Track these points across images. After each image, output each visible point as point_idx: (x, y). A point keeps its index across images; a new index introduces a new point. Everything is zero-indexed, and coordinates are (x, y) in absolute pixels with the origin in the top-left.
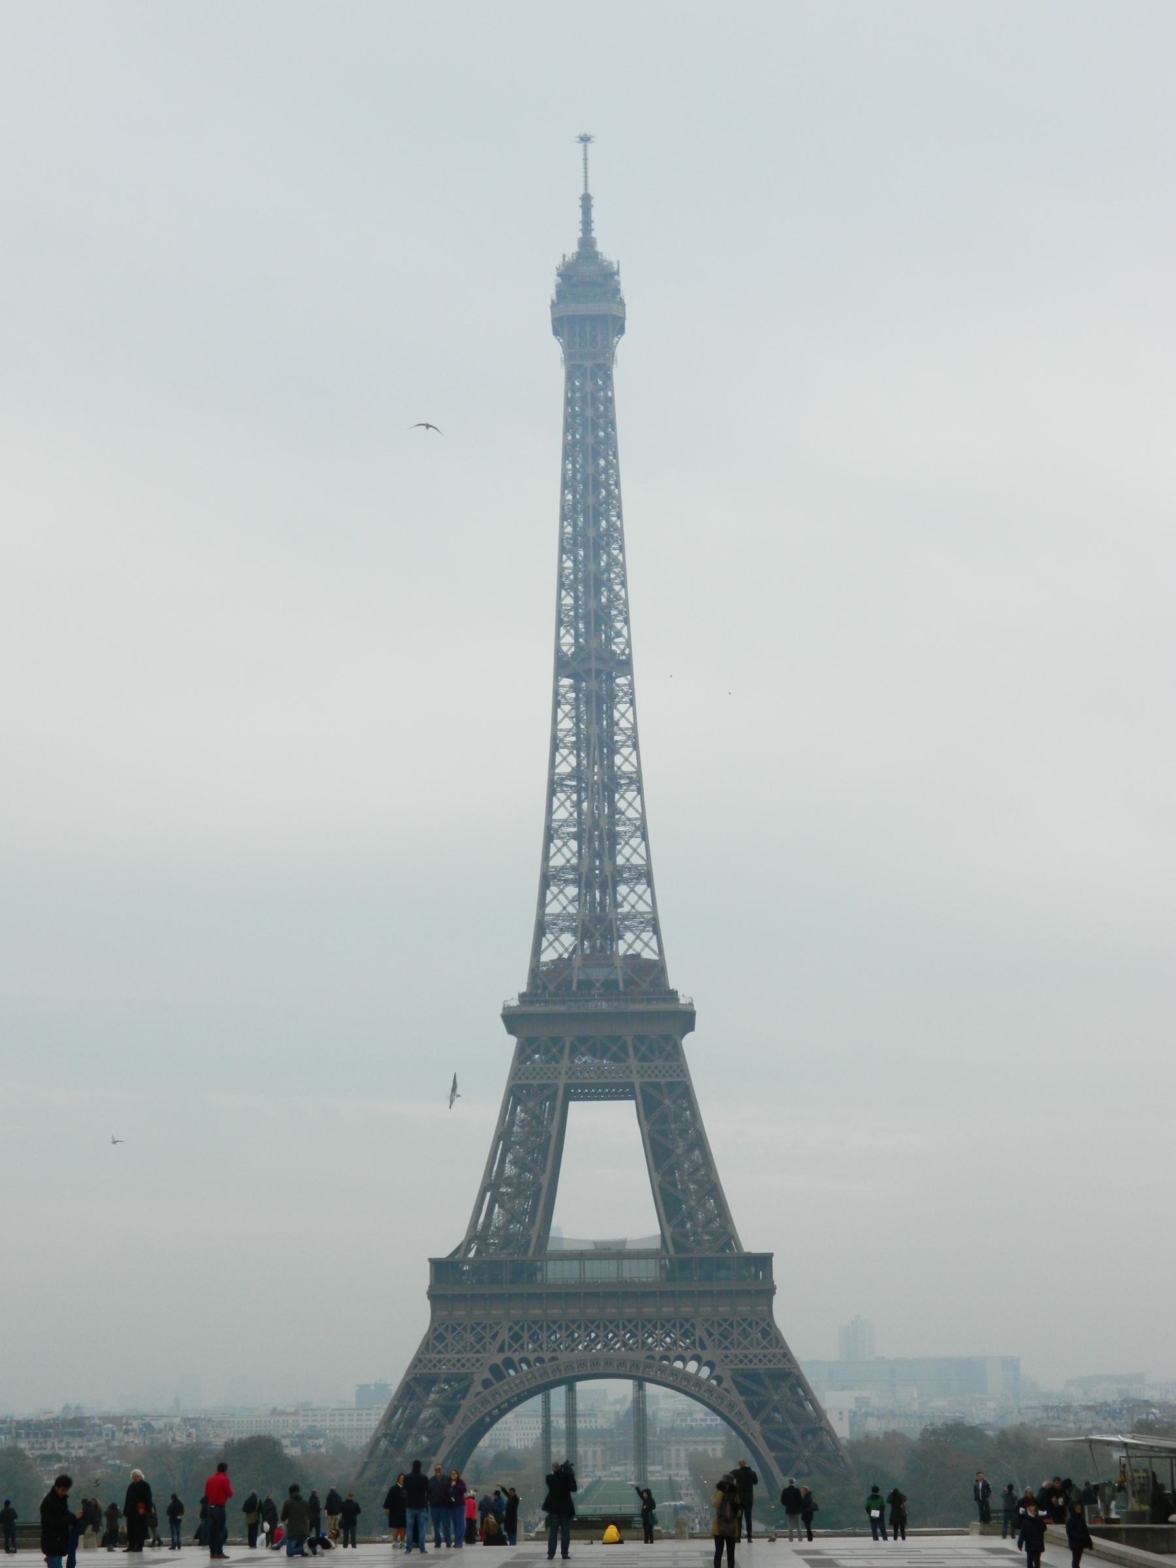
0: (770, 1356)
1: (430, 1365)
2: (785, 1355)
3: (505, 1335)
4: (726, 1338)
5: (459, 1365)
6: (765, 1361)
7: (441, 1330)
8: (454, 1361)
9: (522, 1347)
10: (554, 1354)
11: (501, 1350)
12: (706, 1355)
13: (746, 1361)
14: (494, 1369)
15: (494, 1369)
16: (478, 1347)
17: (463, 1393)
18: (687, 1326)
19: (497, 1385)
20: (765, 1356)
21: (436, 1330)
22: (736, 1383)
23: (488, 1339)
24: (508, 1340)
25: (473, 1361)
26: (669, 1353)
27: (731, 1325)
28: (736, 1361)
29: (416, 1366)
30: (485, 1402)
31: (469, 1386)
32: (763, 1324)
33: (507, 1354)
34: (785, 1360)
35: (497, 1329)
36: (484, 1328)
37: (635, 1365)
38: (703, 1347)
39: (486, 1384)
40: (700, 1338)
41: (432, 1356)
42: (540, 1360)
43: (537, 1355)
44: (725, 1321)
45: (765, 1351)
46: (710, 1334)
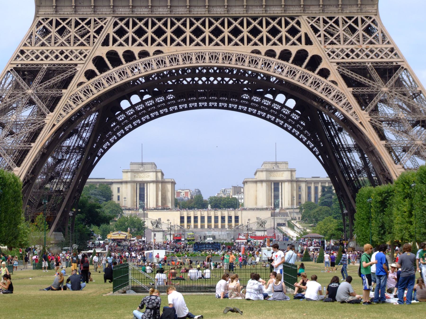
0: (376, 51)
1: (33, 57)
2: (392, 50)
3: (109, 30)
4: (332, 35)
5: (62, 57)
6: (372, 55)
7: (44, 24)
8: (57, 53)
9: (127, 41)
10: (159, 48)
11: (106, 43)
12: (312, 51)
13: (353, 55)
14: (99, 62)
15: (99, 62)
16: (82, 40)
17: (65, 84)
18: (293, 23)
19: (100, 77)
20: (372, 51)
21: (40, 24)
22: (344, 77)
23: (92, 33)
24: (112, 34)
25: (77, 53)
26: (274, 48)
27: (337, 22)
28: (343, 55)
29: (18, 56)
30: (87, 92)
31: (71, 78)
32: (369, 22)
33: (111, 47)
34: (392, 55)
35: (102, 24)
36: (89, 23)
37: (241, 59)
38: (309, 42)
39: (90, 75)
40: (306, 35)
41: (34, 48)
42: (143, 54)
43: (140, 49)
44: (331, 18)
45: (371, 46)
46: (316, 31)
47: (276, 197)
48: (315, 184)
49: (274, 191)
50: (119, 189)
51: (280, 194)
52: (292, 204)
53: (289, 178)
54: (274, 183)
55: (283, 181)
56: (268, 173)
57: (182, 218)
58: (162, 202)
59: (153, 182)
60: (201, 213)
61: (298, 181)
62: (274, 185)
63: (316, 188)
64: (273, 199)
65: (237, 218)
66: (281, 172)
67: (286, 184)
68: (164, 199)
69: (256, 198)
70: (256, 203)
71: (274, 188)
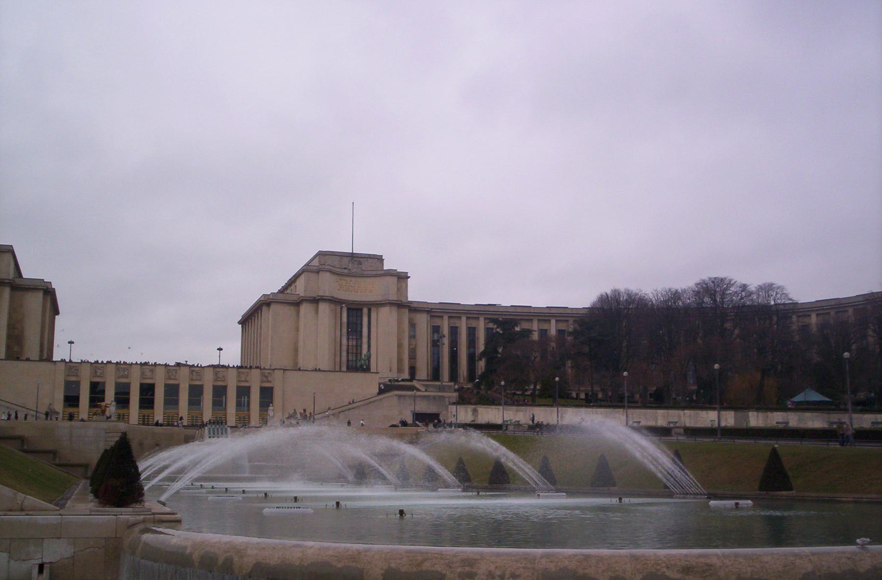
48: (452, 321)
53: (393, 297)
54: (348, 309)
56: (334, 277)
61: (415, 309)
62: (348, 316)
63: (454, 331)
64: (344, 354)
67: (385, 311)
69: (296, 350)
71: (348, 323)
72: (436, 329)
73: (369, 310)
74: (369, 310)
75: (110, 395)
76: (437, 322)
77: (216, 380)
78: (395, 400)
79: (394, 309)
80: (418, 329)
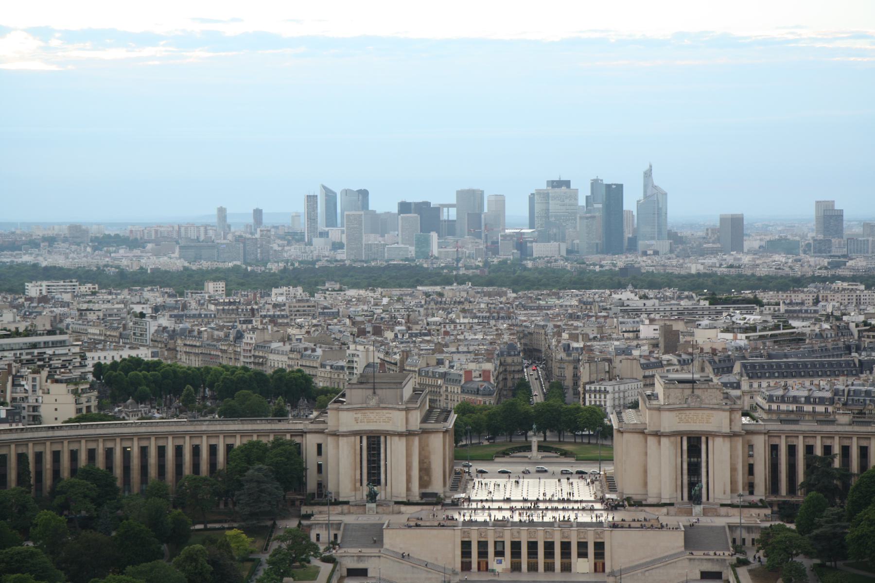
47: (694, 469)
48: (789, 439)
49: (689, 456)
50: (319, 446)
51: (704, 464)
52: (733, 490)
54: (689, 439)
55: (709, 435)
56: (674, 414)
57: (466, 546)
58: (420, 478)
59: (400, 435)
60: (512, 534)
62: (689, 442)
63: (792, 450)
64: (685, 477)
65: (600, 547)
66: (706, 412)
67: (719, 441)
68: (425, 471)
70: (645, 484)
72: (774, 448)
73: (707, 439)
74: (707, 439)
75: (491, 550)
76: (775, 441)
77: (563, 537)
78: (687, 561)
79: (727, 440)
80: (755, 449)
